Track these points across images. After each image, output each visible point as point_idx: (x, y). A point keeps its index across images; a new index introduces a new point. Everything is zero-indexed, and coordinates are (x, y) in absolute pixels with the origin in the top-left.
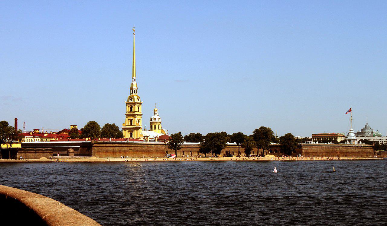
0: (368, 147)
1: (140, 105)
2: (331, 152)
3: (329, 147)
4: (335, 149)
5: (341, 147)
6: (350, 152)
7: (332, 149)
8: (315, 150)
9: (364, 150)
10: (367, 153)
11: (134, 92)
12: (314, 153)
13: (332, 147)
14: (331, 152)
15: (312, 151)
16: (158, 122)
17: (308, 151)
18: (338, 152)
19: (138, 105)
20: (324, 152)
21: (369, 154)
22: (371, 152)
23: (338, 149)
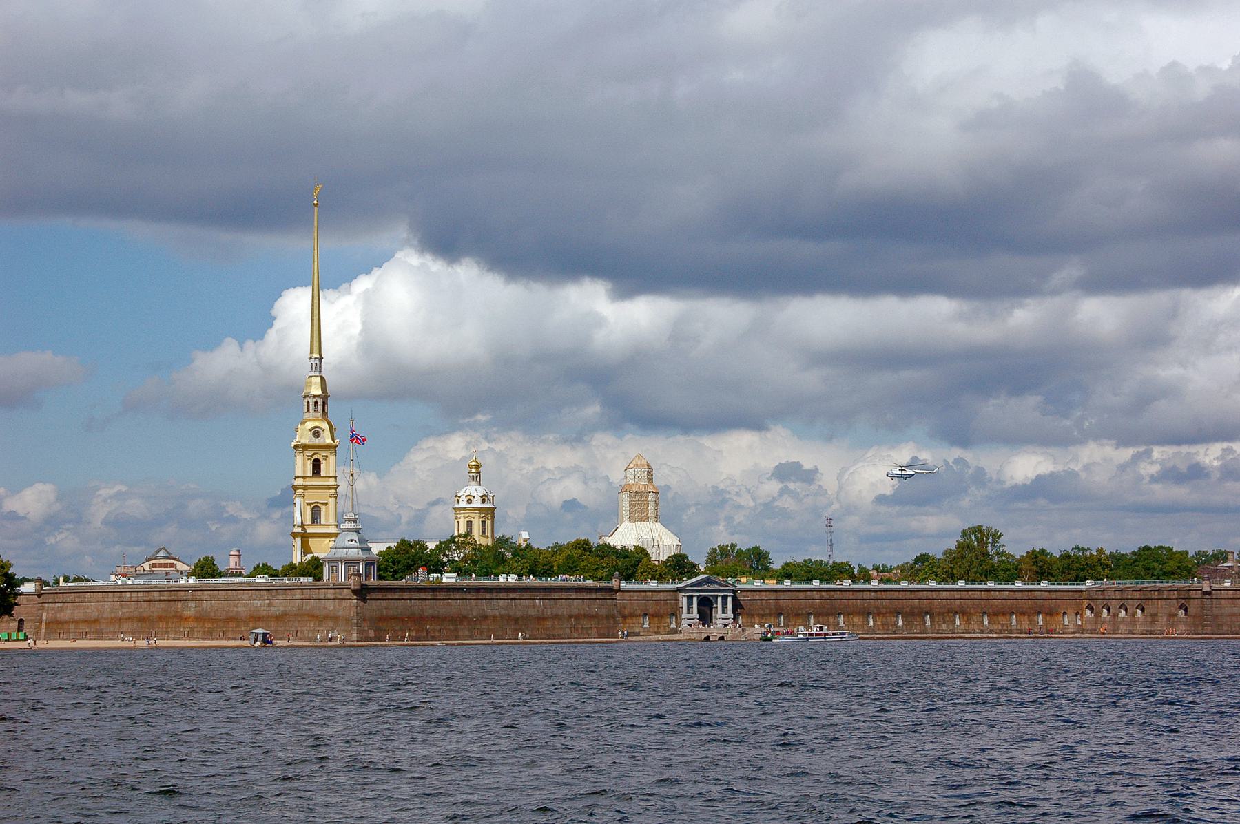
0: (330, 594)
2: (160, 618)
4: (180, 605)
5: (205, 595)
7: (162, 605)
9: (308, 606)
10: (320, 619)
11: (312, 408)
13: (166, 596)
14: (160, 618)
15: (79, 615)
16: (464, 509)
17: (61, 616)
21: (330, 624)
23: (192, 604)
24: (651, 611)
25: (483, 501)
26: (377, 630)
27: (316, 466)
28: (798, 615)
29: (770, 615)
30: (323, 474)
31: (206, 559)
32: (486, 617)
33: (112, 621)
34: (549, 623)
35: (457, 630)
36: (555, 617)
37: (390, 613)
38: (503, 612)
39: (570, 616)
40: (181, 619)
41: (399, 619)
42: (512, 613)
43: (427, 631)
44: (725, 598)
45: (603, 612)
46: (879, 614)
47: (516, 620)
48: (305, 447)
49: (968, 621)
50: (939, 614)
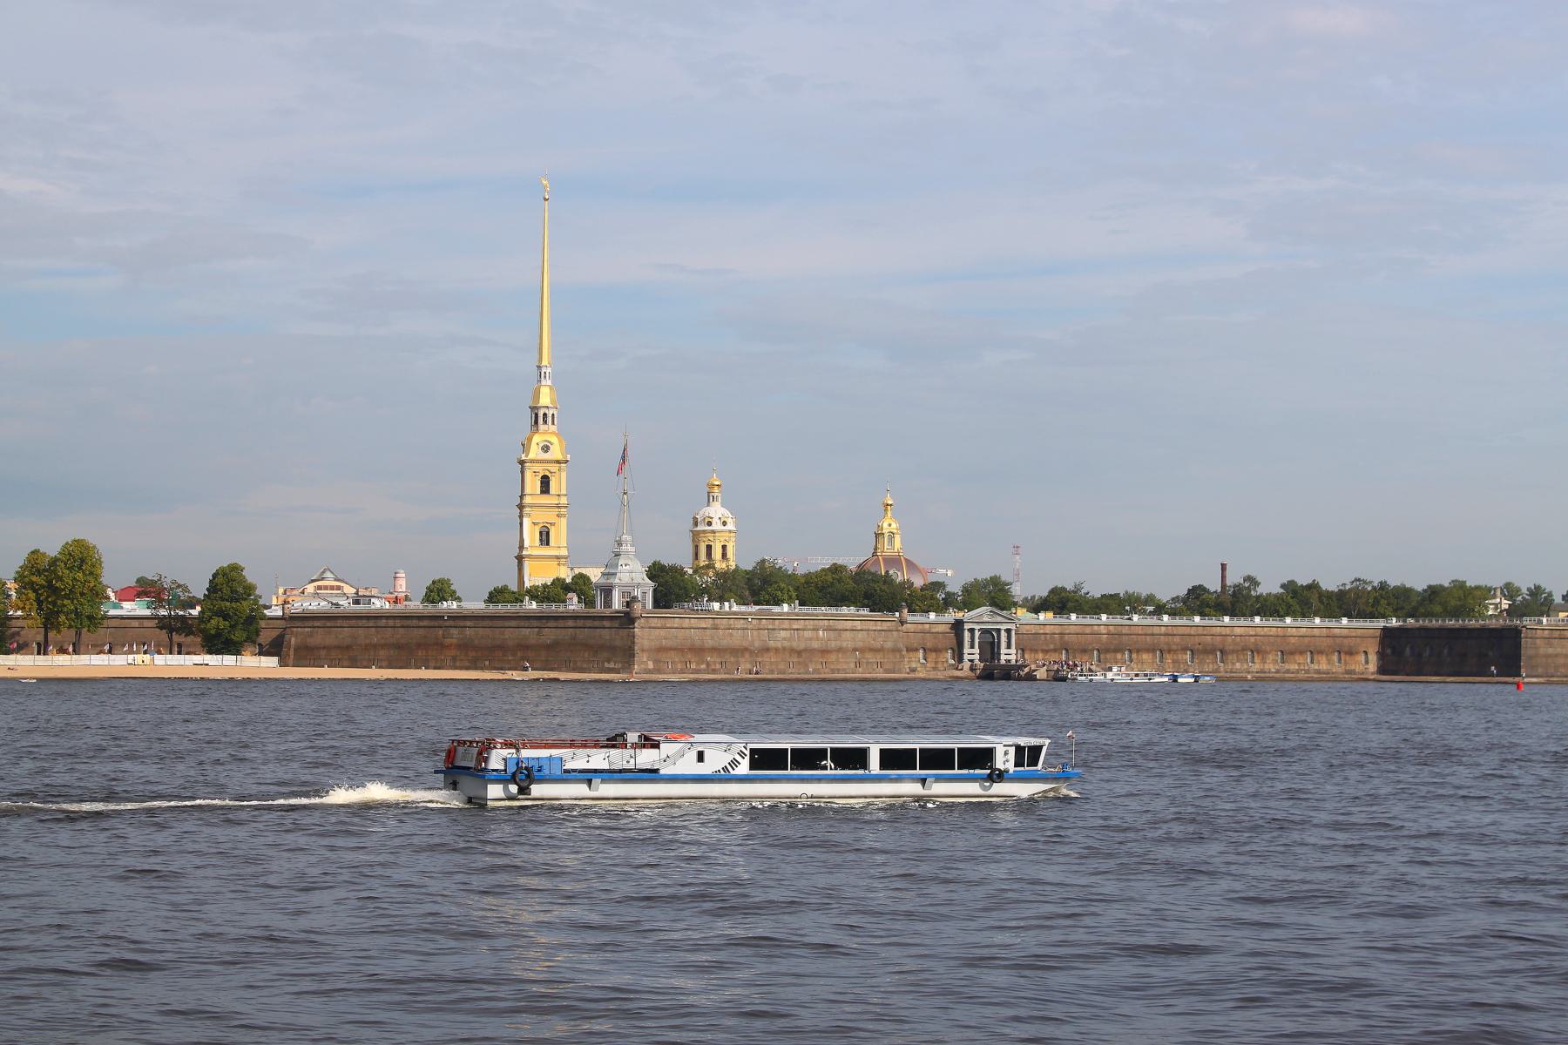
0: (606, 623)
1: (554, 467)
3: (409, 623)
4: (441, 632)
5: (468, 623)
6: (510, 643)
8: (344, 634)
9: (583, 634)
12: (338, 647)
13: (425, 623)
14: (419, 645)
15: (330, 640)
17: (311, 642)
18: (449, 647)
19: (537, 467)
20: (383, 646)
21: (606, 655)
22: (618, 643)
23: (454, 631)
24: (929, 645)
25: (725, 523)
26: (656, 662)
27: (545, 483)
28: (1084, 651)
29: (1055, 650)
30: (552, 491)
31: (441, 581)
32: (768, 650)
33: (367, 647)
34: (833, 657)
35: (738, 663)
36: (839, 650)
37: (669, 643)
38: (786, 644)
39: (855, 650)
40: (441, 646)
41: (679, 650)
42: (794, 644)
43: (708, 664)
44: (1008, 631)
45: (889, 645)
46: (1169, 651)
47: (799, 653)
48: (532, 461)
49: (1264, 661)
50: (1233, 652)
